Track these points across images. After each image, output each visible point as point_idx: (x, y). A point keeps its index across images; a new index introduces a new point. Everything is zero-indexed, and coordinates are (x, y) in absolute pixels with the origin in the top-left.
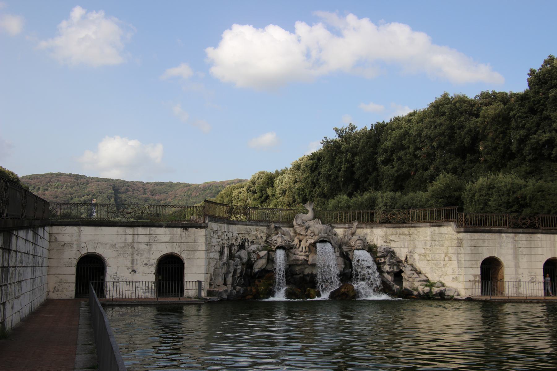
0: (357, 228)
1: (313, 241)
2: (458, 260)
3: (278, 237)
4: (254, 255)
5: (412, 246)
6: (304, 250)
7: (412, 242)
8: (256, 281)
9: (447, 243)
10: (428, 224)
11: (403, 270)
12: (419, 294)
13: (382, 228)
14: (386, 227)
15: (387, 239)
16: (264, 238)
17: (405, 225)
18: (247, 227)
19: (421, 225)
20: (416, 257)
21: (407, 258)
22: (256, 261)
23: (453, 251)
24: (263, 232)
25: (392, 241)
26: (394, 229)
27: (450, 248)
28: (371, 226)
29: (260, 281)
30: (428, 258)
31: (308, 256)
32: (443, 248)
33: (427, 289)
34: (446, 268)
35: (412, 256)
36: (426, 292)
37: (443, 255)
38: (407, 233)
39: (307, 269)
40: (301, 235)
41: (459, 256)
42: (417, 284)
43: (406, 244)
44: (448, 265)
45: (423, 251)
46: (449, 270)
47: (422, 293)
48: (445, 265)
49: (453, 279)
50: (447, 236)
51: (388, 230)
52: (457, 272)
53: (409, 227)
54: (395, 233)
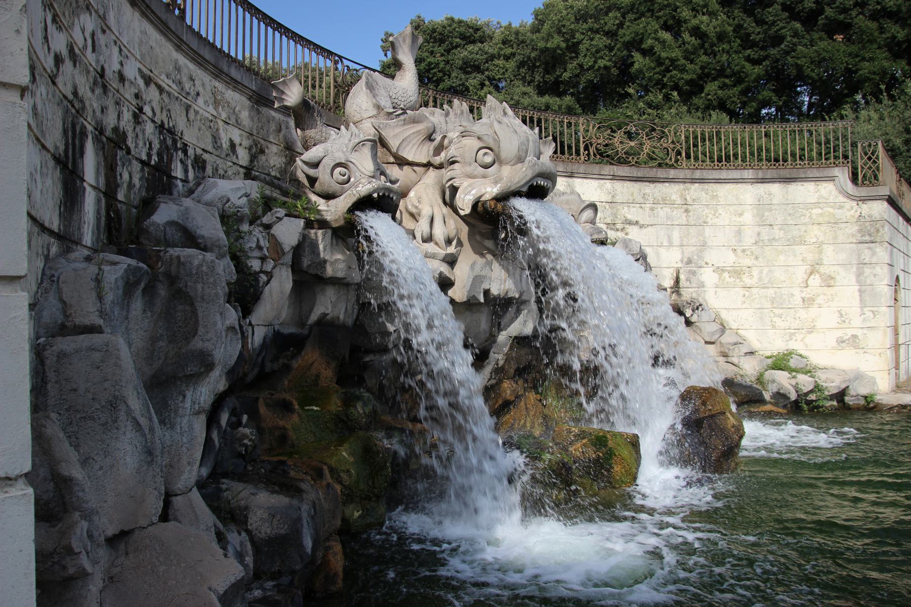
1: (490, 190)
2: (860, 283)
3: (355, 148)
4: (255, 236)
5: (693, 241)
6: (439, 232)
7: (693, 230)
8: (263, 410)
9: (815, 233)
10: (748, 174)
11: (693, 319)
12: (780, 396)
13: (601, 177)
14: (614, 178)
15: (615, 215)
16: (243, 157)
17: (672, 173)
18: (183, 60)
19: (724, 174)
20: (708, 276)
21: (677, 281)
22: (270, 275)
23: (842, 257)
24: (238, 124)
25: (630, 223)
26: (637, 185)
27: (829, 250)
28: (570, 168)
29: (285, 407)
30: (748, 281)
31: (451, 261)
32: (799, 249)
33: (805, 382)
34: (813, 311)
35: (694, 273)
36: (805, 390)
37: (801, 272)
38: (679, 201)
40: (401, 162)
41: (867, 271)
43: (676, 234)
44: (819, 300)
45: (729, 259)
46: (826, 317)
47: (793, 396)
48: (808, 302)
49: (841, 341)
50: (816, 211)
51: (618, 185)
52: (857, 321)
53: (684, 181)
54: (639, 199)
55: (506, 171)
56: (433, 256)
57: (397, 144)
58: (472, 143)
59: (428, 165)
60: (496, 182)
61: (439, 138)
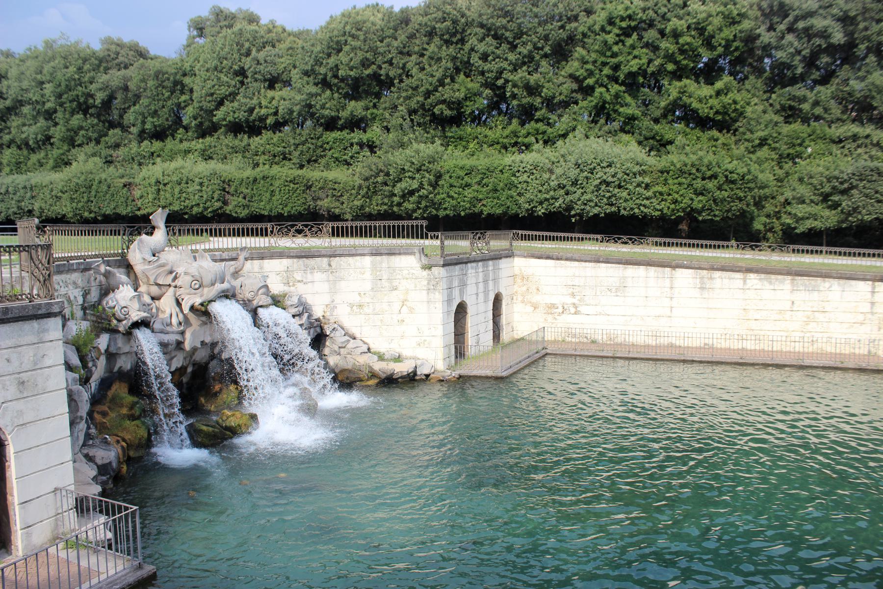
0: (246, 259)
1: (197, 301)
25: (299, 281)
31: (183, 333)
37: (397, 306)
39: (175, 359)
42: (363, 360)
55: (206, 290)
56: (173, 333)
57: (154, 277)
58: (189, 279)
59: (170, 285)
60: (201, 296)
61: (174, 274)
